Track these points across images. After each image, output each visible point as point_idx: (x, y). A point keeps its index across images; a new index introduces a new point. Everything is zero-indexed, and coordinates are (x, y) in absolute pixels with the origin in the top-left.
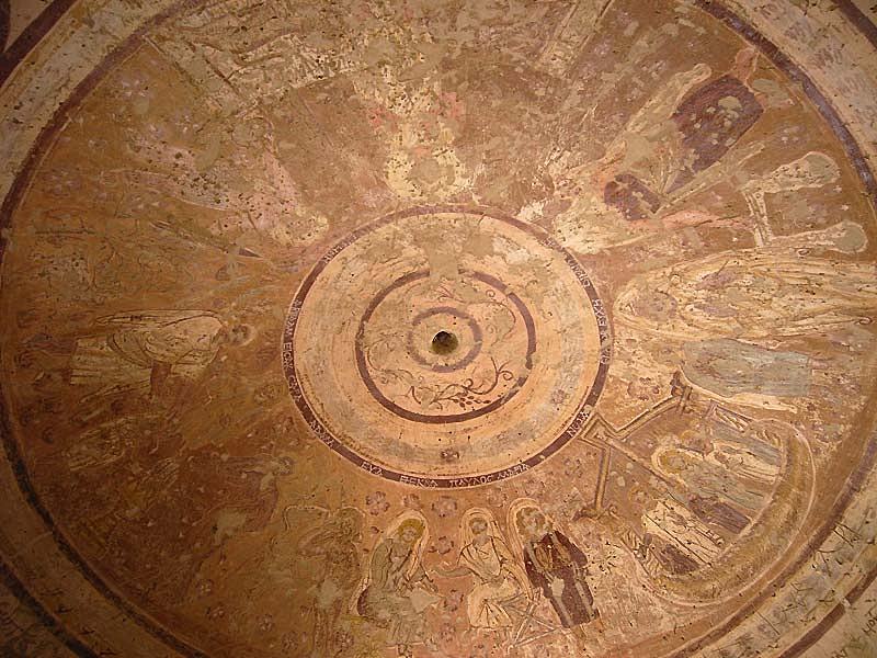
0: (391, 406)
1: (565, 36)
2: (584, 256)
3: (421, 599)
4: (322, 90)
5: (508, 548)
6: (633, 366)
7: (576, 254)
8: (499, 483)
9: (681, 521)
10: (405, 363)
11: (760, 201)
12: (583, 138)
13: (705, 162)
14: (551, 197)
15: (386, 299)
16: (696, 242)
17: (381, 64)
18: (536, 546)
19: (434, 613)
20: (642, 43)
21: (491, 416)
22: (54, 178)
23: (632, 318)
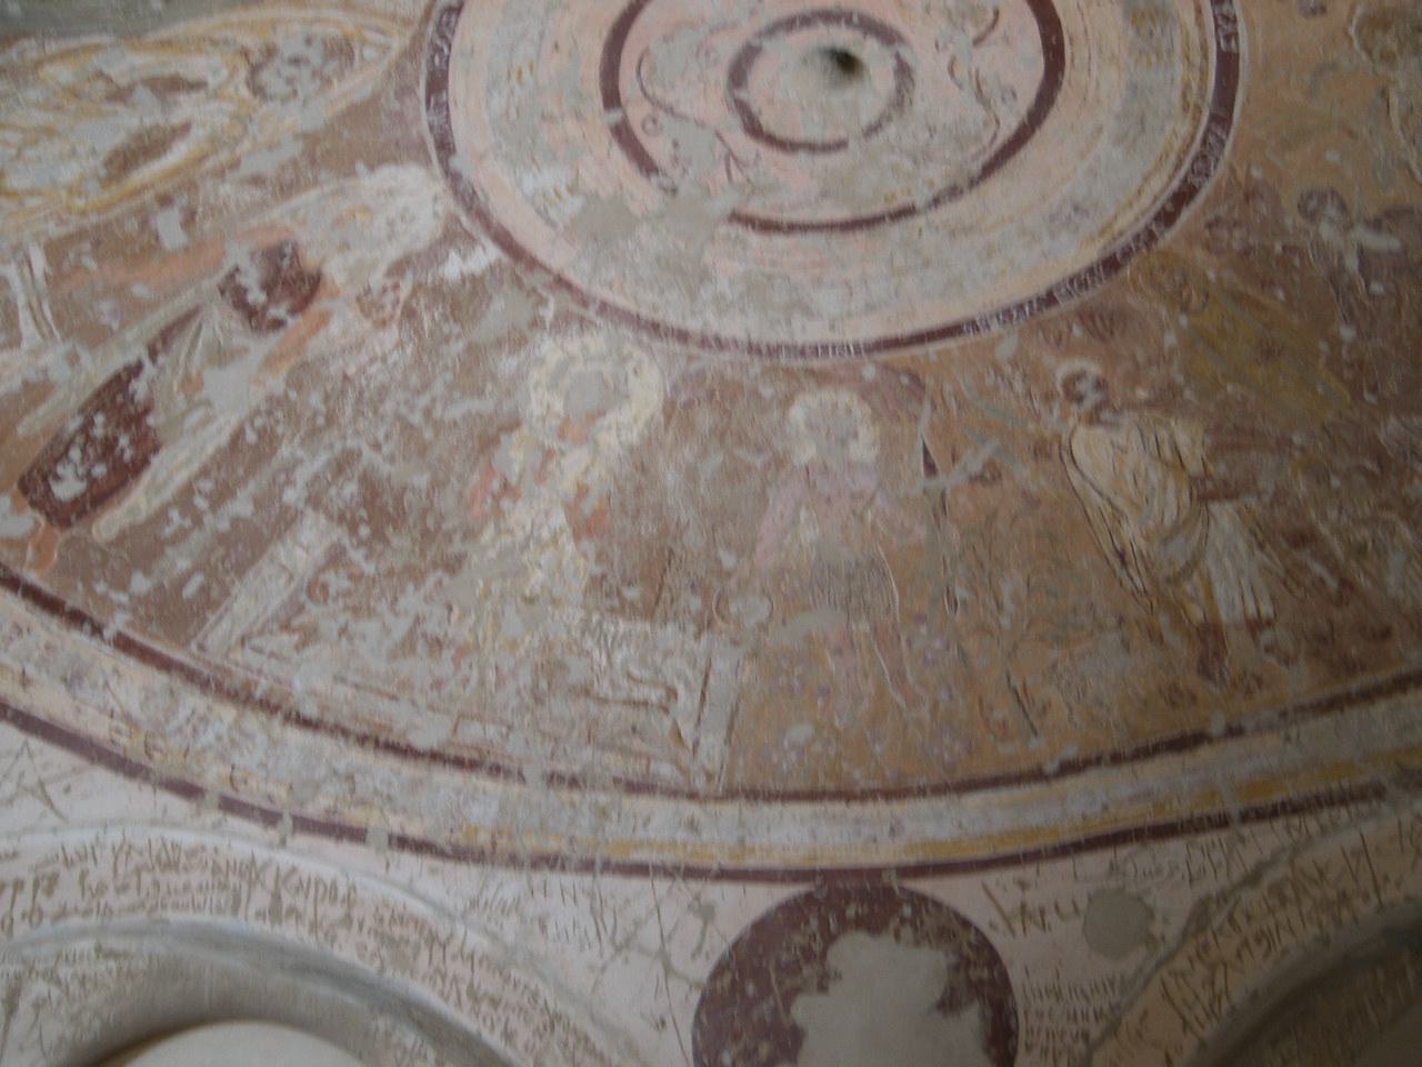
1: (282, 582)
4: (622, 600)
12: (315, 399)
13: (120, 382)
14: (418, 288)
15: (842, 214)
17: (530, 601)
20: (183, 564)
22: (946, 756)
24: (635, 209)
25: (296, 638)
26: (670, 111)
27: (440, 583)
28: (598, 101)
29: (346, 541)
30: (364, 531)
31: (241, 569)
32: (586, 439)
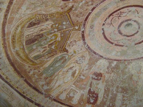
7: (102, 59)
9: (42, 30)
10: (140, 21)
11: (78, 91)
12: (110, 83)
13: (90, 90)
14: (111, 69)
16: (82, 77)
20: (108, 103)
21: (111, 12)
24: (125, 50)
25: (125, 105)
26: (118, 40)
27: (136, 94)
28: (111, 44)
29: (123, 94)
30: (125, 92)
31: (115, 101)
32: (141, 73)
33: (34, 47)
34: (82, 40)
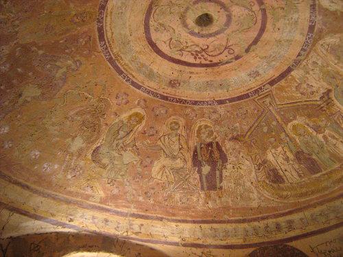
0: (153, 45)
2: (323, 9)
3: (129, 157)
5: (187, 143)
6: (307, 75)
8: (196, 107)
9: (287, 159)
18: (203, 146)
19: (134, 166)
21: (209, 70)
23: (325, 52)
33: (327, 156)
34: (292, 73)
